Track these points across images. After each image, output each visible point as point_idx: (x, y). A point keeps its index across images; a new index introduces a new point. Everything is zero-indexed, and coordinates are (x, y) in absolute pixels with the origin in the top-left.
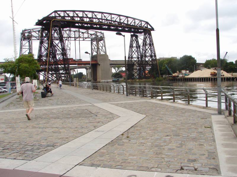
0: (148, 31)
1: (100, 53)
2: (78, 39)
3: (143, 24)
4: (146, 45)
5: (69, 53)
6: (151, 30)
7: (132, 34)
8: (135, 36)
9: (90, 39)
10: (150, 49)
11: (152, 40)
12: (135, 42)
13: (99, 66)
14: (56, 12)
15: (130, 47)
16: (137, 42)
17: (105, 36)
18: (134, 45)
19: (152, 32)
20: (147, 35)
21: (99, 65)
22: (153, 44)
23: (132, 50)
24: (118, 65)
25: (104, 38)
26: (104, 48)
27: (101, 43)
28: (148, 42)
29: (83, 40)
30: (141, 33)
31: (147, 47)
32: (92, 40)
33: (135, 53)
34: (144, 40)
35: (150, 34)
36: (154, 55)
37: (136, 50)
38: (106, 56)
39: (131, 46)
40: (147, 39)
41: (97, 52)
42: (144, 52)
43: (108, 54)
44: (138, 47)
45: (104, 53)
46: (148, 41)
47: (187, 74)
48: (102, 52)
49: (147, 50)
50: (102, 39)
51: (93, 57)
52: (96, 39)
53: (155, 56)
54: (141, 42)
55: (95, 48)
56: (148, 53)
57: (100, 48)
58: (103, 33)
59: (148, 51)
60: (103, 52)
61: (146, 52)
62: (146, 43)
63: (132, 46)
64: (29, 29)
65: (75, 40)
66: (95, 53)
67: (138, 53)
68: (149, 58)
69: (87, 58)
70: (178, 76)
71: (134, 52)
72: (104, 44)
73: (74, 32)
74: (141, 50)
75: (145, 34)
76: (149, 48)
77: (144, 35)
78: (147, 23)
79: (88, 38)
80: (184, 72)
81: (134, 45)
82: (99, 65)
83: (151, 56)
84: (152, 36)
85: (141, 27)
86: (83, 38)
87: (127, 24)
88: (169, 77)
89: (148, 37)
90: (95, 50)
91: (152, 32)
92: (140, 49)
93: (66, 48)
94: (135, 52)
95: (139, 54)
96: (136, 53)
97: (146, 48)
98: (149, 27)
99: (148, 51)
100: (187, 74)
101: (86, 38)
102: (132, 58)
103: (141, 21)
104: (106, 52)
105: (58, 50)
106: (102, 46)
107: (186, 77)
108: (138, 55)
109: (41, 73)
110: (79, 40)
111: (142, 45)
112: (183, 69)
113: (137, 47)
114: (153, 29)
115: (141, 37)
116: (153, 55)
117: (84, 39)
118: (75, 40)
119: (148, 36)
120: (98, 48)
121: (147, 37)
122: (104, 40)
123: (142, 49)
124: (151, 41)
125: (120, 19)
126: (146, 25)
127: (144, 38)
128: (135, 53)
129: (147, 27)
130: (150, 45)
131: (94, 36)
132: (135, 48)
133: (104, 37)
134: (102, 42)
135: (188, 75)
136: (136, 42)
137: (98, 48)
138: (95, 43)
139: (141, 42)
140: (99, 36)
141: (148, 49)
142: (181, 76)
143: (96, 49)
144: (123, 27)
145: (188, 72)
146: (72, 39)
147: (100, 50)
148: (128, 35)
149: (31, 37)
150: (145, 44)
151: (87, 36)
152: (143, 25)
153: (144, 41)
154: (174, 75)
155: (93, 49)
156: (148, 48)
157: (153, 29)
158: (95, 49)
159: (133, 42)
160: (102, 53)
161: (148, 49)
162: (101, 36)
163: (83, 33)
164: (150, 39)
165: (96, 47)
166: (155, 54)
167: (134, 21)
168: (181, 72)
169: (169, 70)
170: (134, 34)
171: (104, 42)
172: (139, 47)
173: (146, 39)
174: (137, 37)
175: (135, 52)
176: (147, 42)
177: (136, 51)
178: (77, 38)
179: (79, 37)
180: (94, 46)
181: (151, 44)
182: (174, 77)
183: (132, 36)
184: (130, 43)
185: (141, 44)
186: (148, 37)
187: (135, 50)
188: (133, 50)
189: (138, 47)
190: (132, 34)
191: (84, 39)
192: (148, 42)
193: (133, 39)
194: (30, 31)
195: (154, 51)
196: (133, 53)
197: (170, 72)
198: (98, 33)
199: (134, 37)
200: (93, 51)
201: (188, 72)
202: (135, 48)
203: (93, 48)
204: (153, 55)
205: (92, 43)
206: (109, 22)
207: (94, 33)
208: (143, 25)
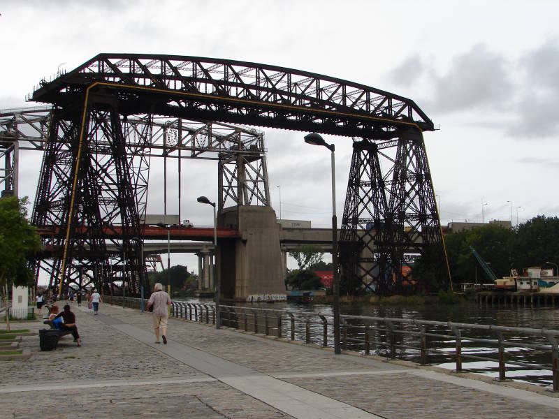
1: (248, 204)
2: (176, 153)
5: (143, 200)
6: (425, 130)
7: (359, 139)
8: (366, 150)
9: (216, 155)
10: (417, 193)
11: (426, 161)
12: (368, 167)
13: (242, 245)
14: (103, 58)
15: (350, 184)
16: (376, 168)
17: (265, 147)
18: (365, 178)
19: (426, 135)
20: (408, 146)
21: (245, 242)
22: (428, 176)
23: (357, 194)
24: (306, 246)
25: (263, 152)
26: (261, 186)
27: (252, 168)
29: (194, 156)
30: (387, 136)
31: (408, 187)
32: (223, 159)
33: (366, 206)
34: (397, 162)
35: (419, 143)
36: (433, 214)
37: (371, 194)
38: (267, 210)
39: (354, 183)
40: (408, 159)
41: (238, 200)
43: (274, 203)
45: (261, 204)
46: (411, 165)
47: (548, 281)
48: (255, 198)
49: (407, 194)
50: (256, 153)
51: (224, 216)
52: (237, 154)
53: (435, 216)
54: (386, 167)
55: (230, 183)
56: (411, 205)
57: (250, 185)
58: (262, 135)
59: (412, 201)
60: (258, 197)
61: (403, 201)
62: (404, 173)
63: (358, 180)
64: (9, 111)
65: (165, 155)
66: (230, 203)
67: (376, 206)
68: (414, 223)
69: (204, 218)
70: (514, 288)
71: (362, 201)
72: (261, 173)
73: (164, 127)
74: (388, 195)
75: (402, 143)
76: (417, 188)
77: (399, 145)
78: (410, 104)
79: (210, 149)
80: (534, 273)
81: (365, 178)
82: (245, 242)
83: (422, 217)
84: (424, 149)
85: (389, 119)
86: (193, 149)
87: (342, 108)
88: (485, 289)
89: (411, 153)
90: (230, 192)
91: (426, 135)
92: (383, 191)
93: (133, 183)
94: (366, 200)
95: (381, 207)
96: (371, 206)
97: (403, 187)
98: (416, 117)
99: (412, 201)
100: (548, 281)
101: (202, 150)
102: (356, 220)
103: (389, 96)
104: (267, 201)
105: (105, 187)
106: (254, 179)
107: (544, 290)
108: (377, 211)
109: (42, 263)
110: (179, 157)
111: (391, 178)
112: (533, 264)
113: (373, 185)
114: (429, 126)
115: (388, 154)
116: (429, 212)
117: (196, 152)
118: (165, 155)
119: (411, 146)
120: (242, 186)
121: (408, 153)
122: (262, 158)
123: (392, 193)
124: (423, 164)
125: (319, 90)
126: (405, 112)
127: (398, 154)
128: (366, 206)
129: (410, 118)
130: (419, 178)
131: (228, 145)
132: (367, 189)
133: (263, 148)
134: (256, 164)
135: (552, 284)
136: (372, 168)
137: (242, 186)
138: (231, 167)
139: (386, 167)
140: (247, 146)
141: (413, 194)
142: (525, 286)
143: (235, 190)
144: (330, 116)
145: (550, 272)
146: (154, 151)
147: (249, 193)
148: (344, 145)
149: (14, 140)
150: (400, 175)
151: (206, 144)
152: (396, 109)
153: (400, 163)
154: (499, 282)
155: (226, 188)
156: (413, 188)
157: (429, 126)
158: (230, 186)
159: (362, 168)
160: (255, 202)
161: (413, 194)
162: (254, 143)
163: (192, 132)
164: (418, 159)
165: (235, 183)
166: (434, 209)
167: (364, 98)
168: (527, 274)
169: (486, 265)
170: (365, 140)
171: (264, 165)
172: (382, 184)
173: (405, 159)
174: (374, 150)
175: (366, 200)
176: (407, 169)
177: (370, 199)
178: (172, 149)
179: (180, 146)
180: (230, 177)
181: (423, 176)
182: (502, 289)
183: (357, 148)
184: (352, 170)
185: (388, 175)
186: (411, 153)
187: (367, 195)
188: (362, 194)
189: (377, 183)
190: (359, 139)
191: (196, 152)
193: (363, 157)
194: (11, 117)
196: (361, 206)
197: (489, 272)
198: (242, 134)
199: (366, 152)
200: (224, 193)
201: (550, 272)
203: (225, 183)
204: (429, 212)
205: (221, 169)
206: (282, 99)
207: (231, 135)
208: (396, 109)
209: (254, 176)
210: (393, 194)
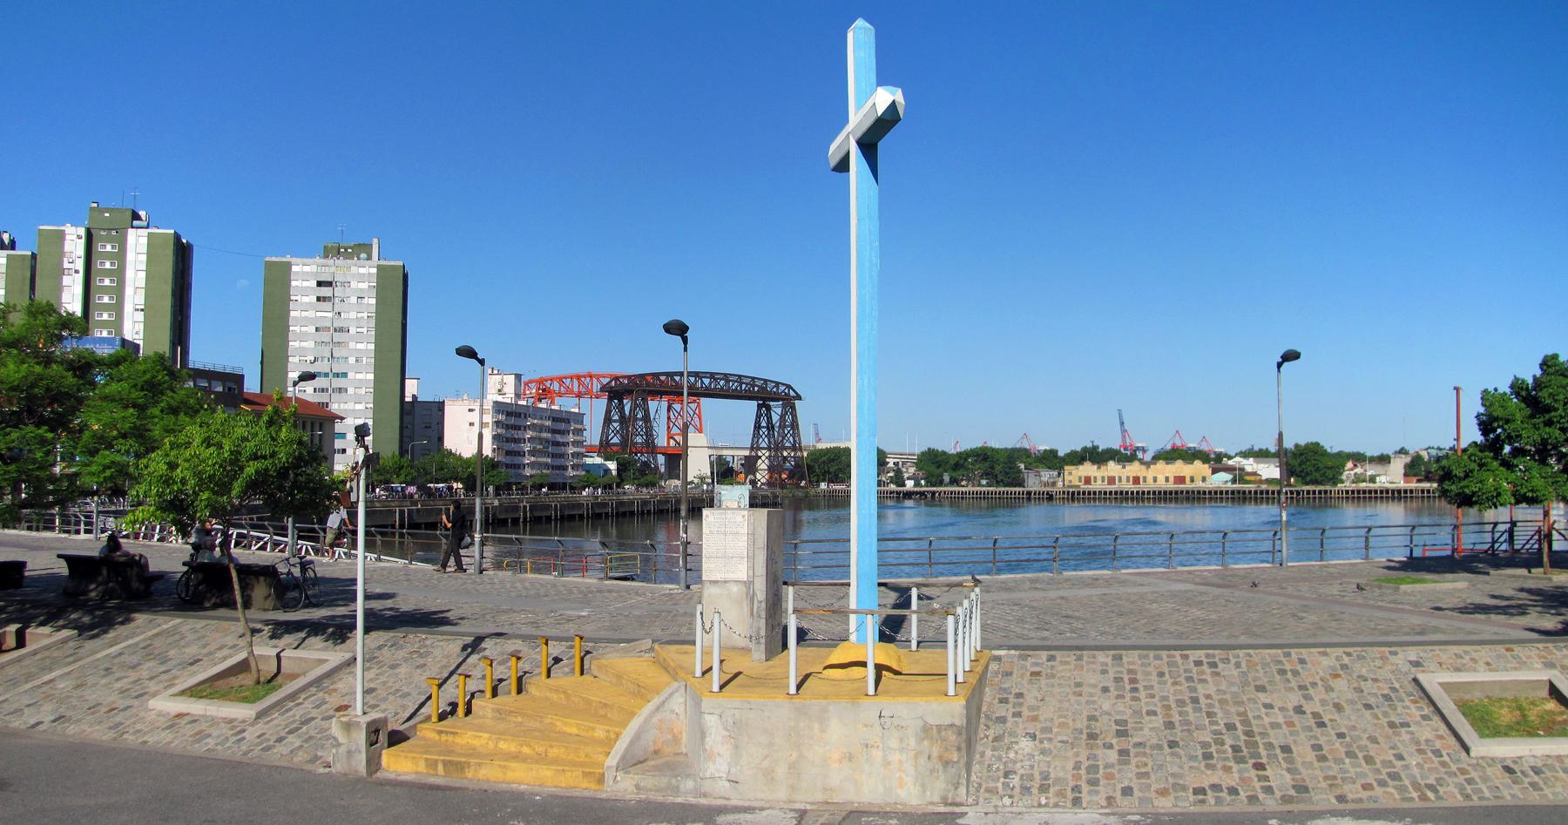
0: (789, 400)
3: (782, 388)
4: (785, 427)
8: (764, 407)
16: (770, 418)
18: (764, 424)
22: (797, 425)
35: (793, 407)
39: (757, 427)
42: (780, 439)
44: (770, 427)
54: (775, 418)
75: (784, 407)
78: (789, 387)
81: (764, 424)
83: (794, 448)
95: (772, 440)
96: (766, 440)
98: (792, 393)
108: (770, 442)
113: (768, 428)
114: (799, 397)
115: (777, 409)
132: (764, 430)
134: (693, 406)
148: (755, 403)
153: (782, 417)
157: (799, 397)
174: (769, 408)
181: (795, 425)
183: (759, 407)
189: (770, 427)
195: (800, 439)
202: (764, 430)
203: (672, 416)
209: (692, 413)
210: (778, 433)
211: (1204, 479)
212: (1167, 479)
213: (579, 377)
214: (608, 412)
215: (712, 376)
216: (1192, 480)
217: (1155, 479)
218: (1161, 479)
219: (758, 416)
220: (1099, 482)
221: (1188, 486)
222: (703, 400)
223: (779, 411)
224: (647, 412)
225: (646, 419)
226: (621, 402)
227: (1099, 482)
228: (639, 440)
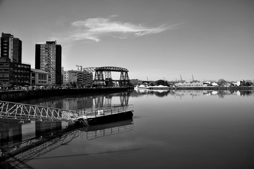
0: (126, 72)
16: (123, 75)
28: (126, 76)
35: (127, 73)
39: (121, 76)
44: (123, 76)
54: (124, 75)
75: (126, 73)
78: (126, 69)
114: (128, 71)
115: (124, 73)
134: (110, 73)
139: (124, 75)
148: (120, 72)
150: (125, 76)
157: (128, 71)
174: (123, 73)
181: (127, 76)
183: (121, 73)
189: (123, 76)
192: (126, 76)
211: (202, 85)
212: (195, 85)
213: (90, 68)
214: (96, 74)
215: (113, 67)
216: (200, 85)
217: (193, 85)
218: (194, 85)
219: (121, 75)
220: (182, 86)
221: (199, 87)
222: (111, 72)
223: (125, 74)
224: (102, 73)
225: (102, 75)
226: (98, 72)
227: (182, 86)
228: (101, 79)
